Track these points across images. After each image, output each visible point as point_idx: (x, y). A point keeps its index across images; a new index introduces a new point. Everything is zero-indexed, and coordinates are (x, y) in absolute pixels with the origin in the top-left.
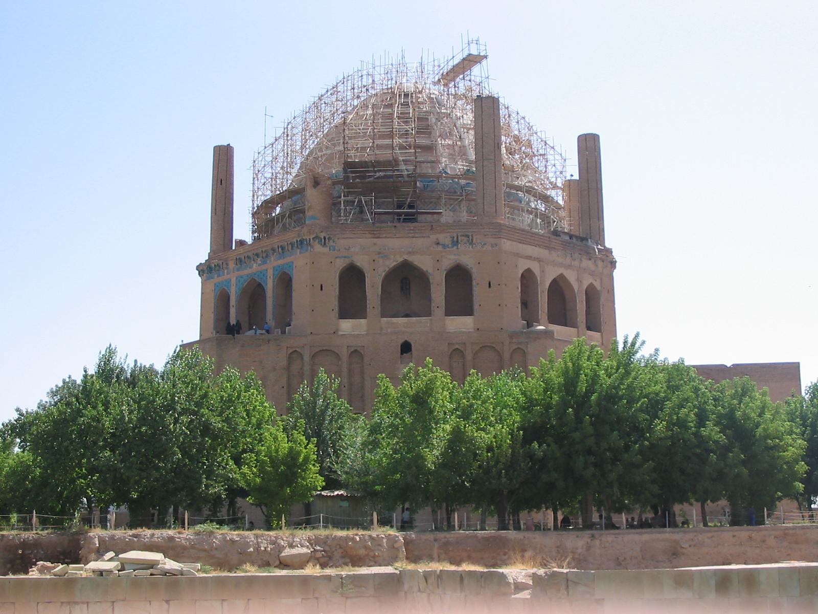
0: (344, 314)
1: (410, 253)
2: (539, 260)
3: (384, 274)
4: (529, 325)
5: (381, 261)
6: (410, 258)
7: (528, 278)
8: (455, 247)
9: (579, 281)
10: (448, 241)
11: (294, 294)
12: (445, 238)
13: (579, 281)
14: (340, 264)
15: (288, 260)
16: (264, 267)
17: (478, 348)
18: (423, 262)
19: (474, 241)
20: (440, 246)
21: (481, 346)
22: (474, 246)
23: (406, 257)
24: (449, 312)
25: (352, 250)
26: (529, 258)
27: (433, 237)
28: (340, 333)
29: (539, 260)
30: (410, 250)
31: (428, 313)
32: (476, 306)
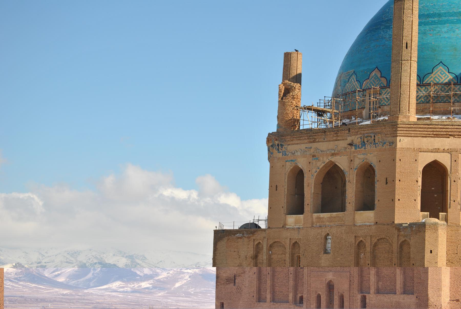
1: (333, 155)
3: (316, 174)
5: (314, 162)
8: (364, 147)
12: (357, 139)
14: (289, 166)
17: (376, 240)
19: (376, 141)
20: (353, 147)
21: (378, 238)
22: (377, 145)
25: (296, 154)
26: (437, 151)
29: (450, 151)
30: (333, 152)
31: (343, 209)
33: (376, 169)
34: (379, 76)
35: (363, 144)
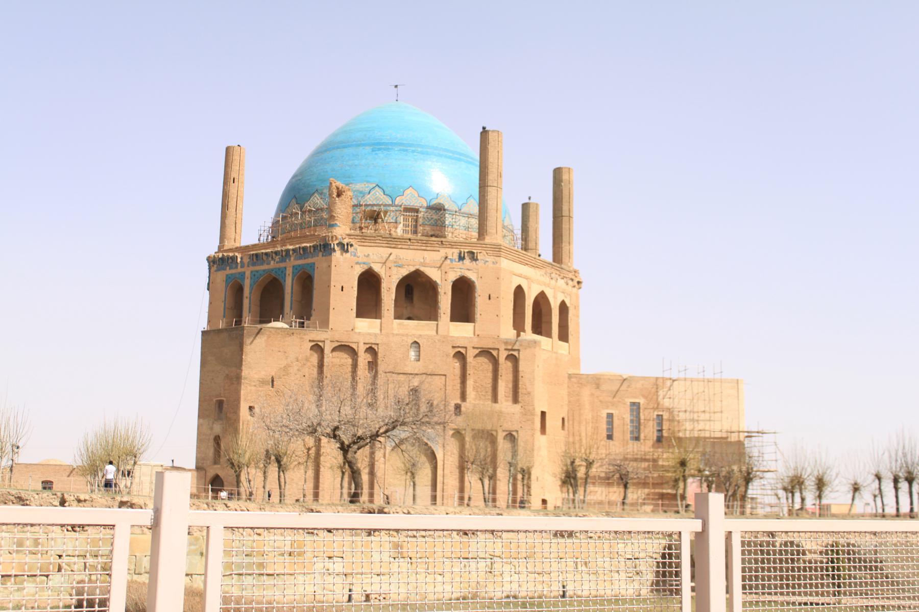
0: (359, 315)
2: (527, 278)
4: (518, 335)
6: (422, 269)
7: (519, 293)
9: (555, 298)
10: (456, 256)
11: (315, 292)
13: (555, 298)
14: (359, 270)
15: (310, 260)
16: (282, 265)
18: (434, 274)
23: (417, 267)
24: (453, 319)
27: (443, 251)
28: (357, 331)
32: (477, 316)
33: (477, 284)
34: (416, 195)
35: (461, 258)
